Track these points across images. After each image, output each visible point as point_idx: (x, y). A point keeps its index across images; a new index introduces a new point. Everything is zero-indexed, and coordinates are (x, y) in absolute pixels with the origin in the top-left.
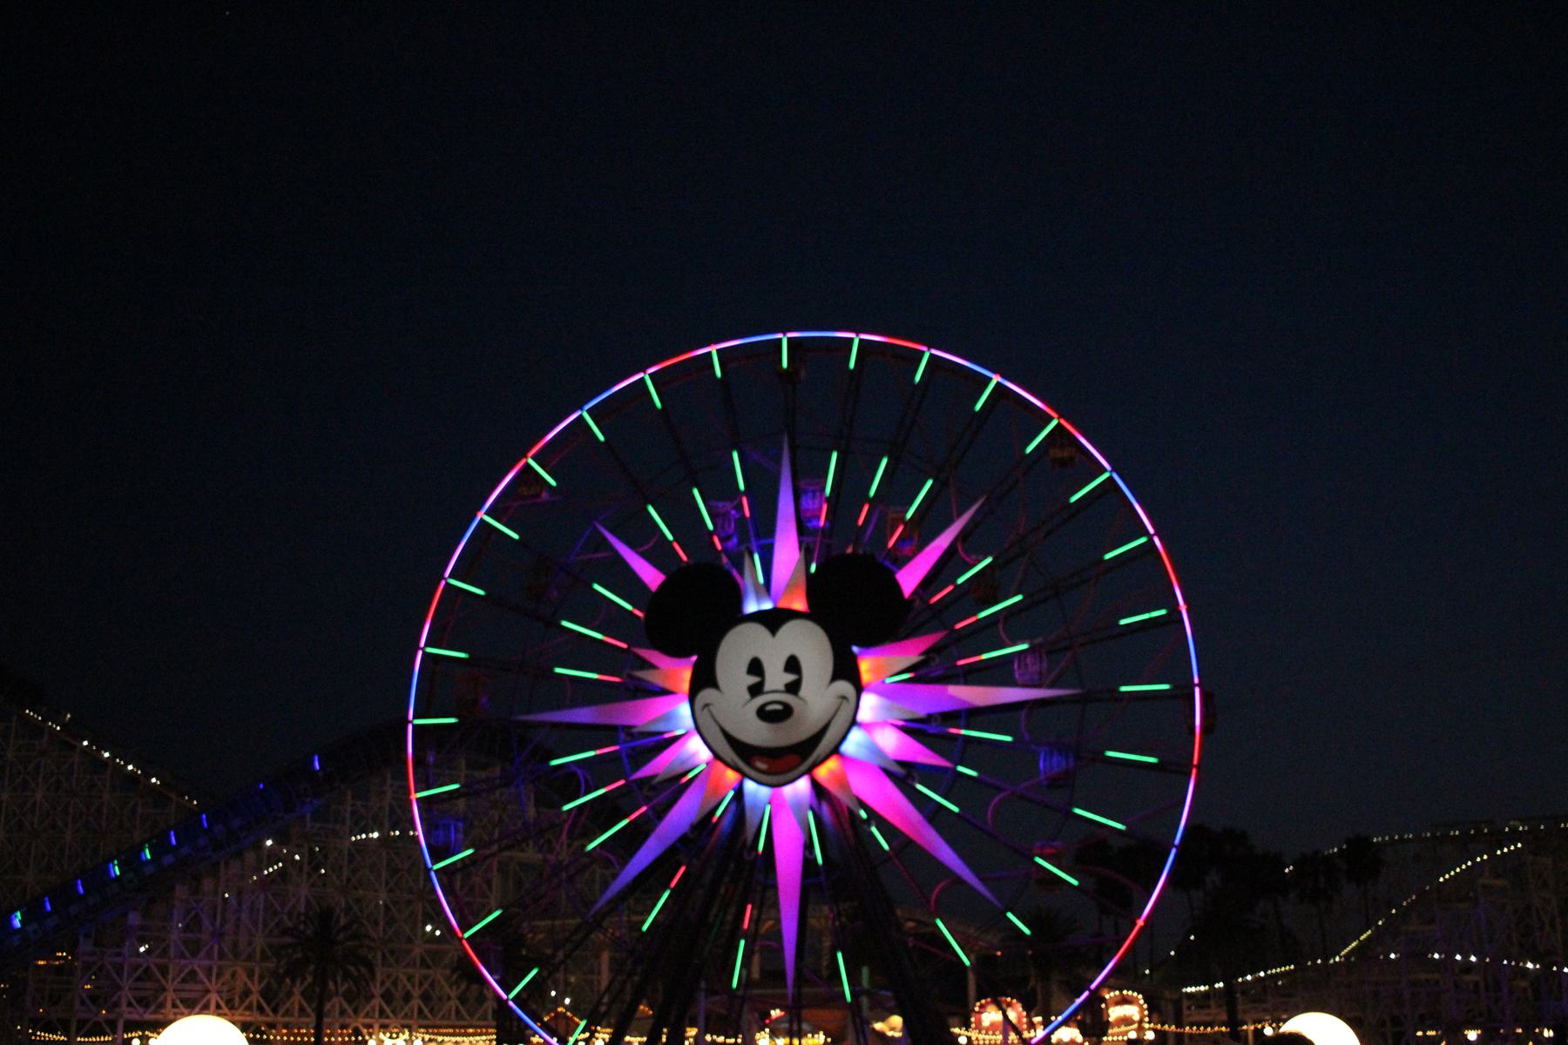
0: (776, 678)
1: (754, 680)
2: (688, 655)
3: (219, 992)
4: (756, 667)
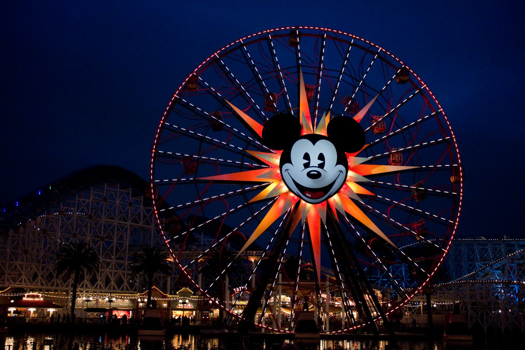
0: (315, 162)
1: (307, 161)
2: (277, 148)
3: (25, 276)
4: (307, 156)
